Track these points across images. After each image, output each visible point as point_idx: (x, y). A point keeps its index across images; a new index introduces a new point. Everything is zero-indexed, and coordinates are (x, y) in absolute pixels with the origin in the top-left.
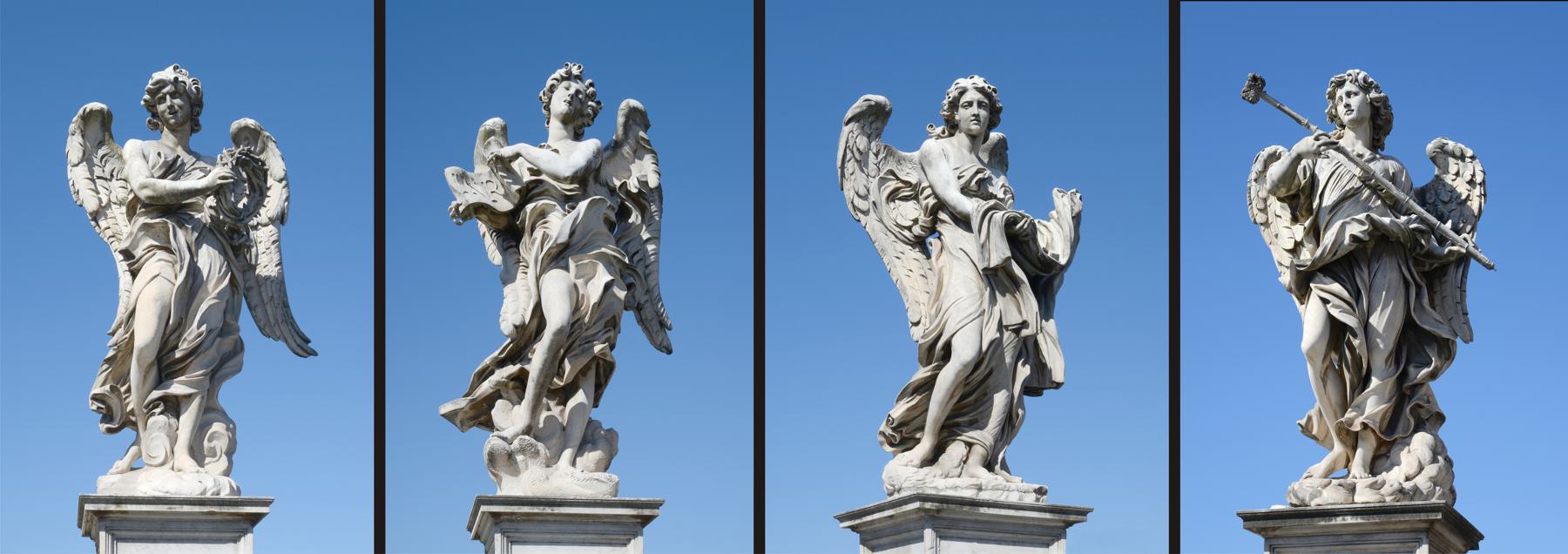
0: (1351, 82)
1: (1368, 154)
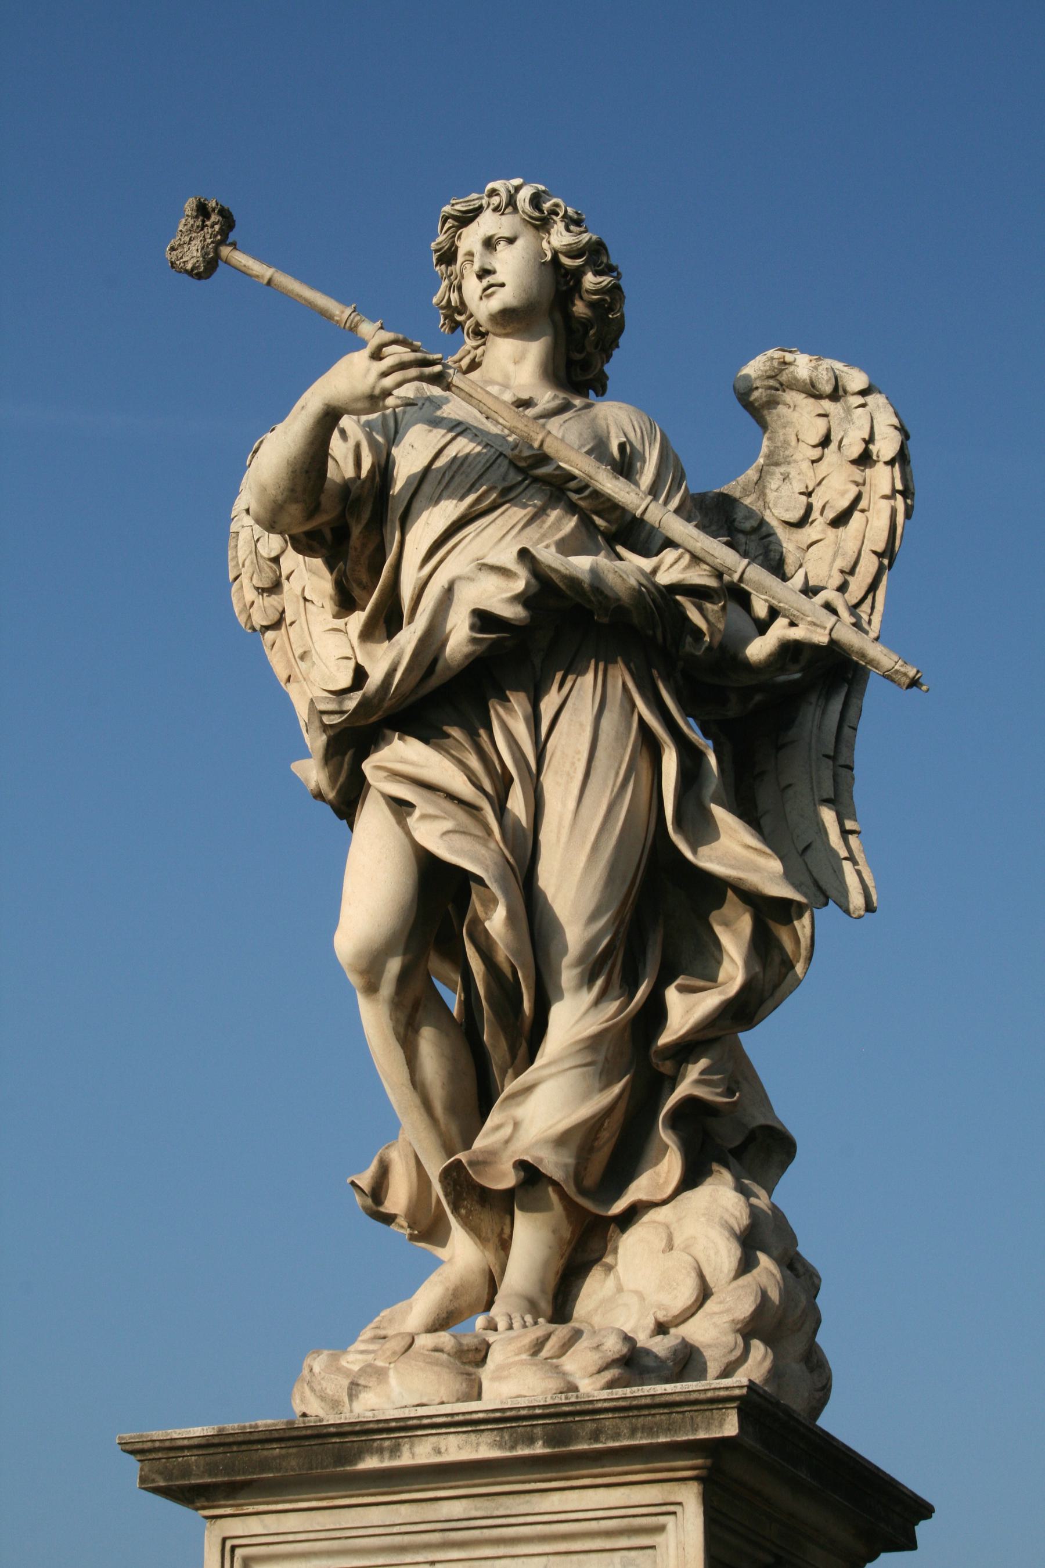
1: (546, 397)
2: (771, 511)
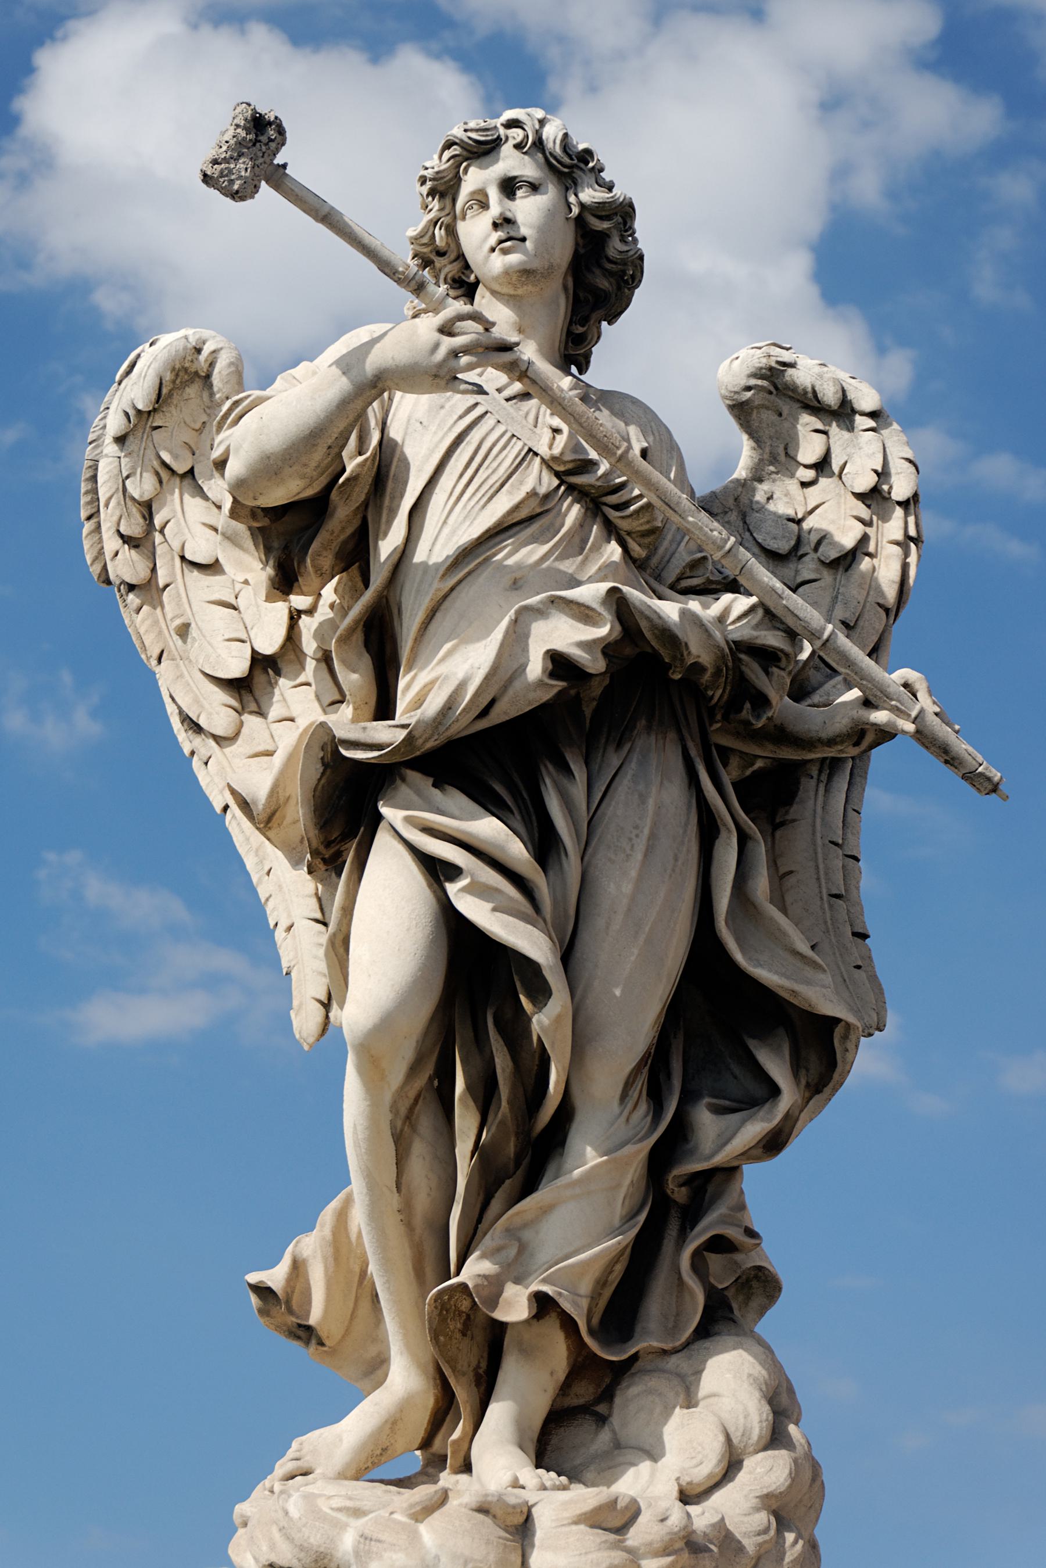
0: (518, 146)
2: (751, 534)
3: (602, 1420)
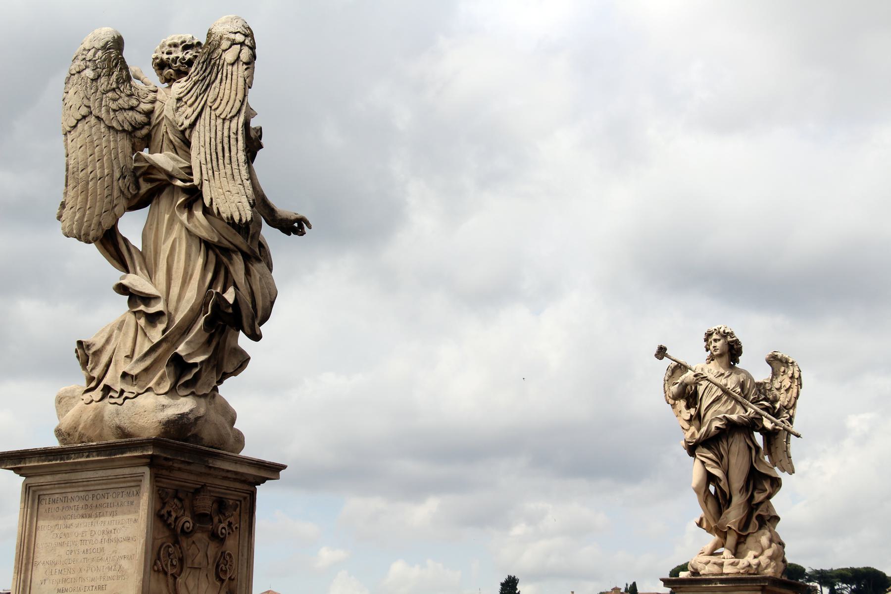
3: (745, 543)
